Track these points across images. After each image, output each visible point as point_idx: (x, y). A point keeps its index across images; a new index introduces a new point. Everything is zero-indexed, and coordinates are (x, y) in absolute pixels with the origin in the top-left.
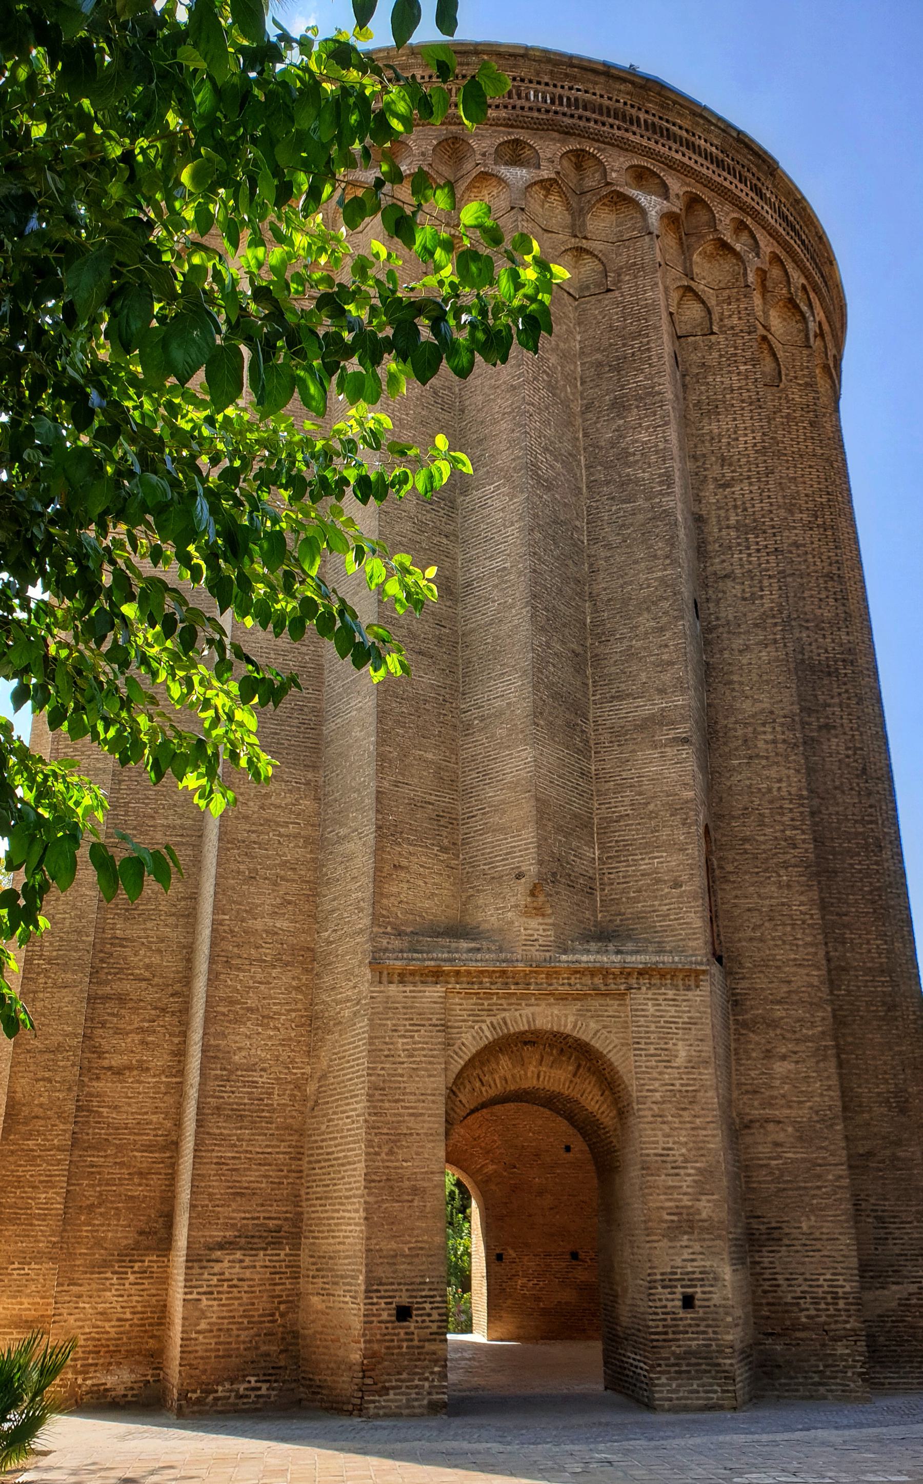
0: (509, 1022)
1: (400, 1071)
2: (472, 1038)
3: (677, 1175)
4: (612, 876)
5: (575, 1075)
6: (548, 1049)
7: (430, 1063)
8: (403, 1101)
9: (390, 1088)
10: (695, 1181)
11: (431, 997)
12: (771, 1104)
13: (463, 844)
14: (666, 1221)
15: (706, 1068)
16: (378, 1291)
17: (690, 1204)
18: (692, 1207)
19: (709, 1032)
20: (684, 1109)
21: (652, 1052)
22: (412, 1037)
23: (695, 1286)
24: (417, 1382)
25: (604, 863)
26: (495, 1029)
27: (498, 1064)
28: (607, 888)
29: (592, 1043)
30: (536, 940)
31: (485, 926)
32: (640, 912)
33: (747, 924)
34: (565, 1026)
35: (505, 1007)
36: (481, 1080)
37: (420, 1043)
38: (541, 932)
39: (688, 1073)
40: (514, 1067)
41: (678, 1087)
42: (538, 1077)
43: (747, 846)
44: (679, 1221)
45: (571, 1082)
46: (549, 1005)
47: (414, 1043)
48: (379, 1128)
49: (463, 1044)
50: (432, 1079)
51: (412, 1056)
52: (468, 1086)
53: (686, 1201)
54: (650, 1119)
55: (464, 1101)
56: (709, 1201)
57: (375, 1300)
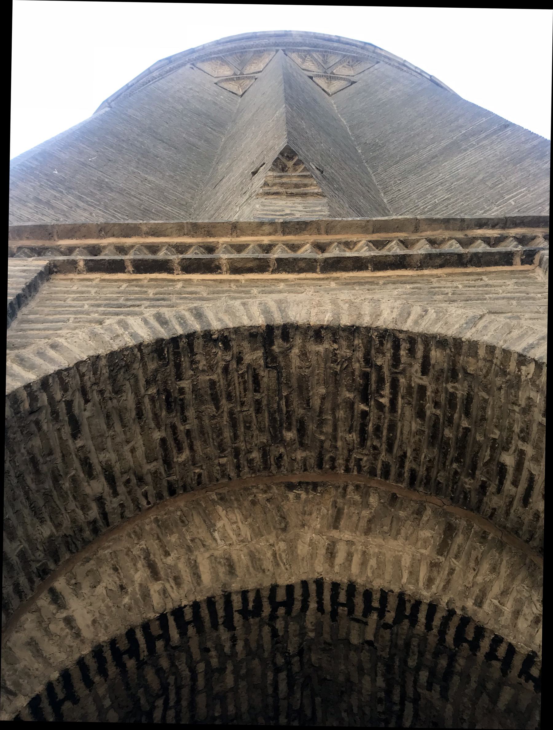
5: (443, 548)
27: (211, 527)
40: (257, 534)
42: (331, 553)
45: (434, 565)
52: (109, 580)
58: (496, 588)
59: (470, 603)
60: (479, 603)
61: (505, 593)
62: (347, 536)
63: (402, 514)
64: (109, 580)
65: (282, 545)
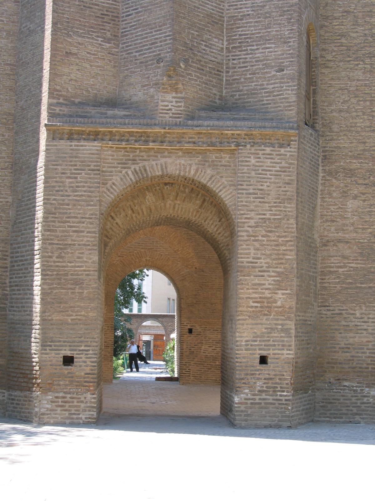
0: (148, 168)
1: (66, 202)
2: (120, 180)
3: (263, 276)
4: (235, 62)
5: (201, 207)
6: (182, 189)
7: (89, 196)
8: (69, 222)
9: (60, 213)
10: (274, 281)
11: (90, 150)
12: (343, 230)
13: (122, 37)
14: (252, 307)
15: (290, 203)
16: (50, 346)
17: (270, 296)
18: (271, 298)
19: (294, 178)
20: (271, 232)
21: (251, 191)
22: (76, 178)
23: (269, 350)
24: (75, 404)
25: (230, 52)
26: (137, 173)
27: (145, 198)
28: (231, 71)
29: (208, 185)
30: (170, 109)
31: (135, 99)
32: (253, 90)
33: (338, 99)
34: (190, 171)
35: (145, 158)
36: (132, 209)
37: (81, 182)
38: (174, 104)
39: (276, 207)
41: (268, 216)
42: (174, 208)
43: (343, 40)
44: (261, 307)
45: (198, 211)
46: (179, 157)
47: (77, 182)
48: (51, 240)
49: (114, 184)
50: (89, 207)
51: (76, 191)
52: (123, 214)
53: (267, 294)
54: (246, 238)
55: (120, 223)
56: (283, 294)
57: (48, 351)
58: (210, 218)
59: (203, 221)
60: (205, 222)
61: (211, 219)
62: (178, 202)
63: (193, 195)
64: (123, 214)
65: (163, 204)
